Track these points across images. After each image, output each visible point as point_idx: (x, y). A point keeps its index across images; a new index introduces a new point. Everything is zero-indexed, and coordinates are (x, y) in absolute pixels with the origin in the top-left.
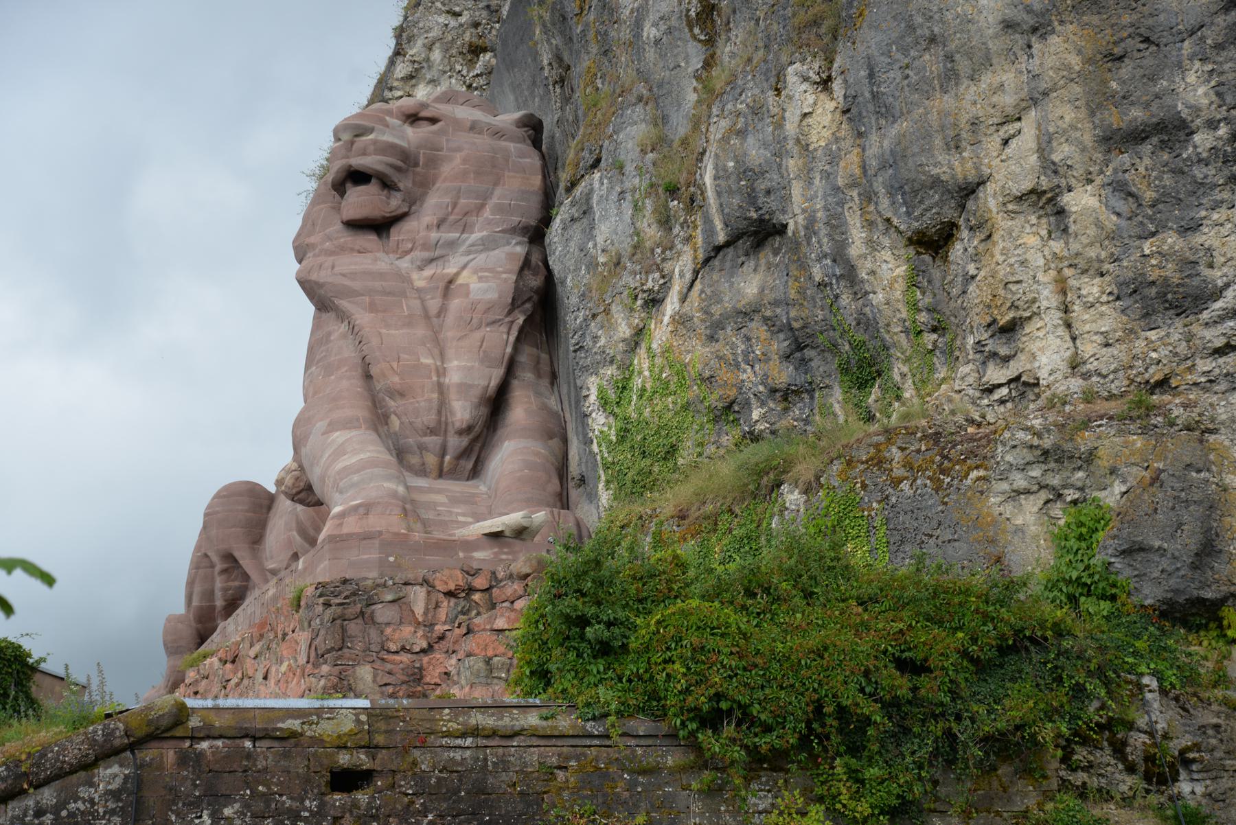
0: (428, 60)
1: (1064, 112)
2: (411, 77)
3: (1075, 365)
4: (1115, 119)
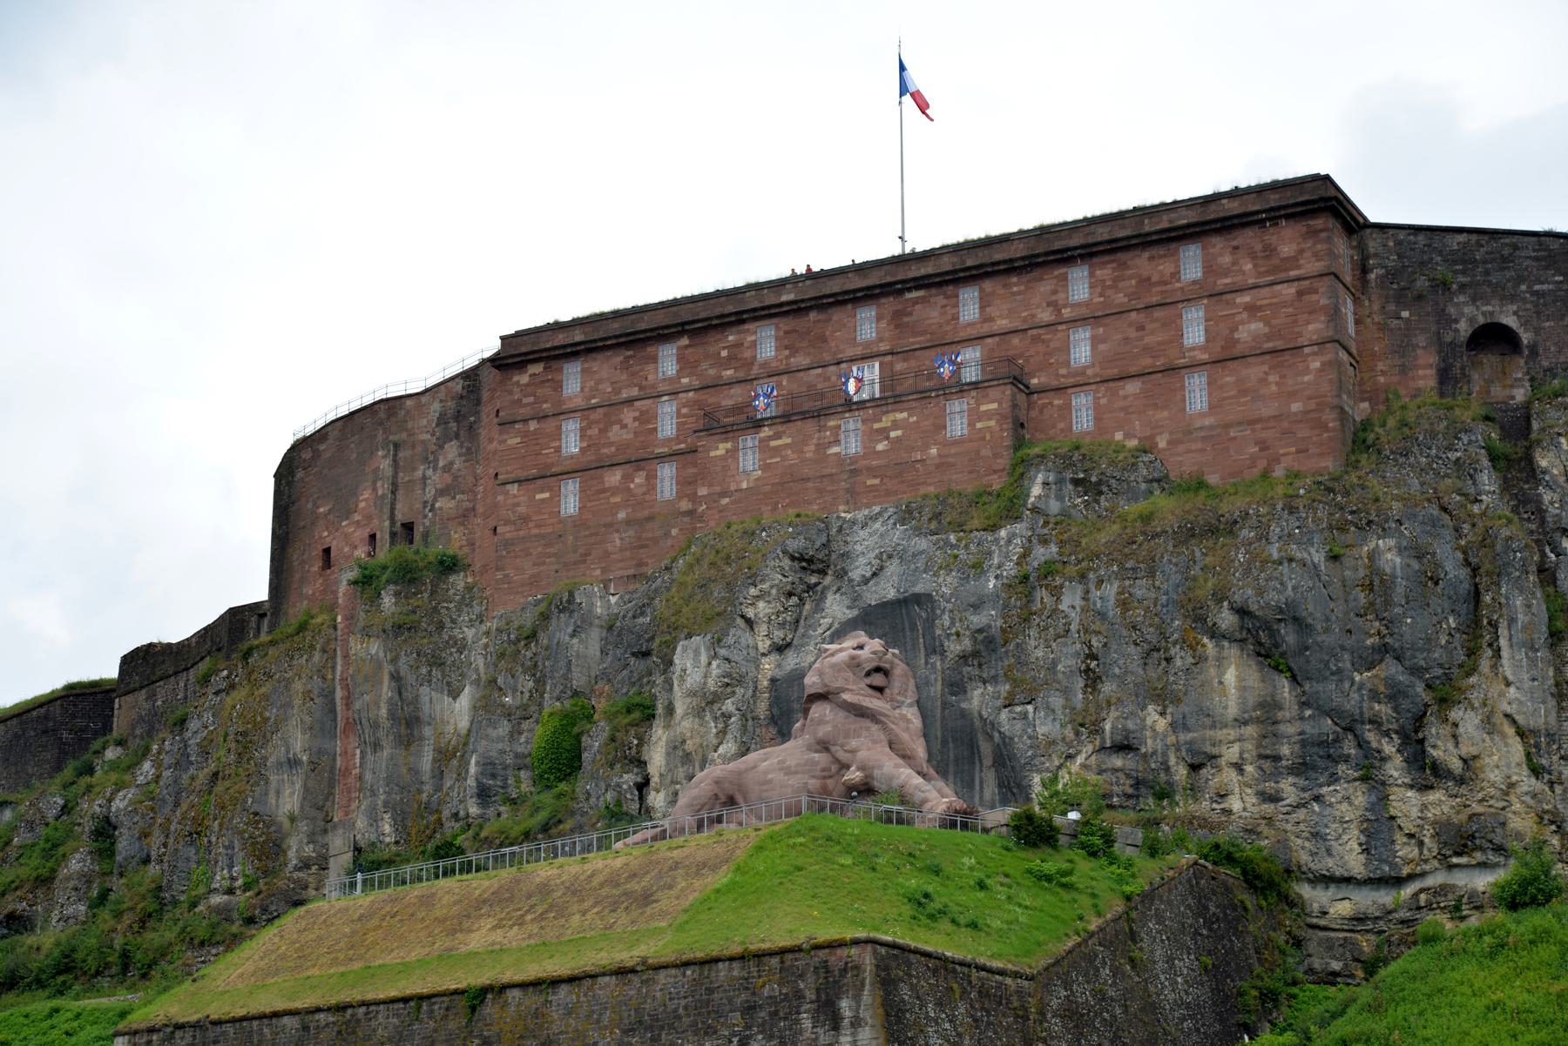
1: (1249, 746)
3: (1245, 809)
4: (1262, 751)
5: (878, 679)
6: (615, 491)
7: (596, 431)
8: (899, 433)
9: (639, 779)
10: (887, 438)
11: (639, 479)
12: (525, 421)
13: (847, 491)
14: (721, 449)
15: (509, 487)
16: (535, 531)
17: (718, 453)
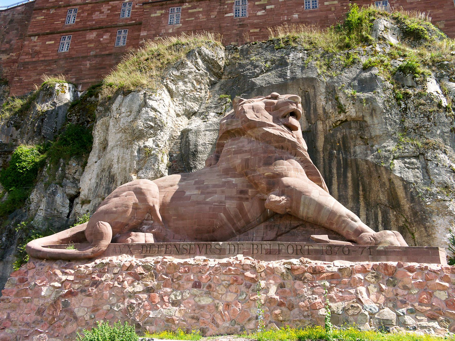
0: (187, 76)
2: (178, 76)
5: (293, 121)
6: (91, 41)
7: (86, 14)
8: (273, 6)
9: (72, 192)
10: (265, 9)
11: (106, 36)
12: (48, 9)
13: (237, 35)
14: (158, 13)
15: (32, 38)
16: (43, 59)
17: (156, 15)
